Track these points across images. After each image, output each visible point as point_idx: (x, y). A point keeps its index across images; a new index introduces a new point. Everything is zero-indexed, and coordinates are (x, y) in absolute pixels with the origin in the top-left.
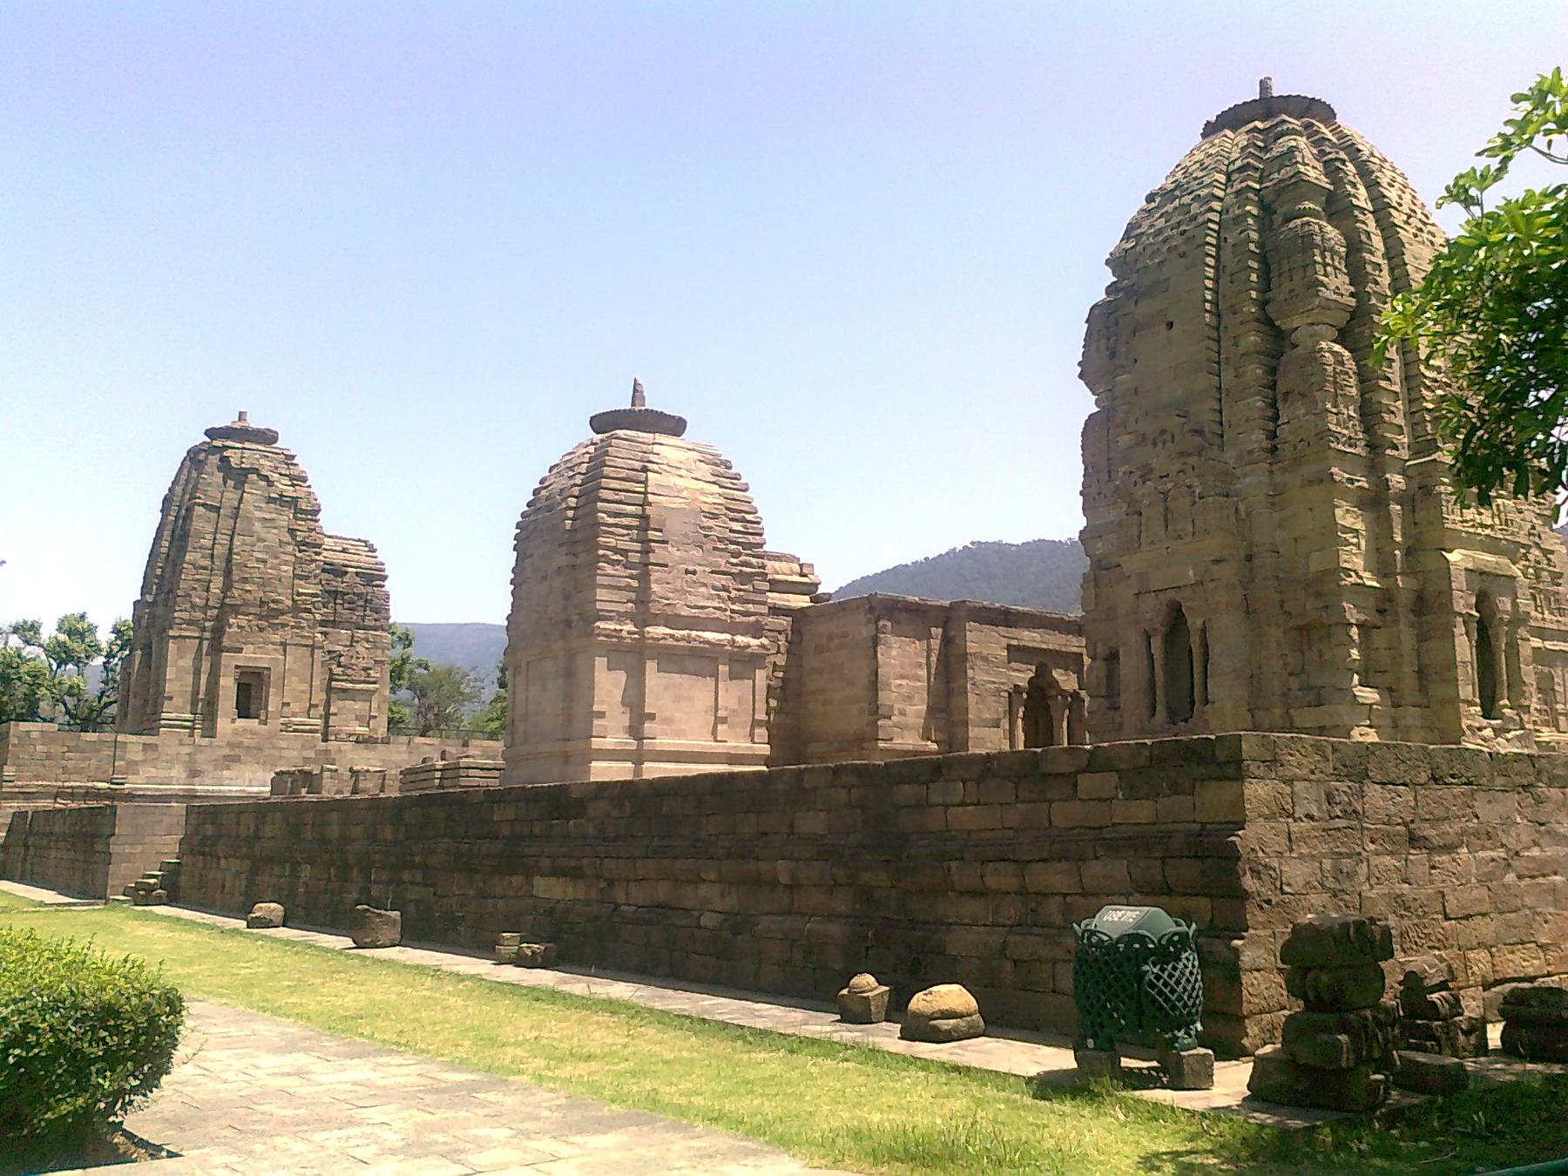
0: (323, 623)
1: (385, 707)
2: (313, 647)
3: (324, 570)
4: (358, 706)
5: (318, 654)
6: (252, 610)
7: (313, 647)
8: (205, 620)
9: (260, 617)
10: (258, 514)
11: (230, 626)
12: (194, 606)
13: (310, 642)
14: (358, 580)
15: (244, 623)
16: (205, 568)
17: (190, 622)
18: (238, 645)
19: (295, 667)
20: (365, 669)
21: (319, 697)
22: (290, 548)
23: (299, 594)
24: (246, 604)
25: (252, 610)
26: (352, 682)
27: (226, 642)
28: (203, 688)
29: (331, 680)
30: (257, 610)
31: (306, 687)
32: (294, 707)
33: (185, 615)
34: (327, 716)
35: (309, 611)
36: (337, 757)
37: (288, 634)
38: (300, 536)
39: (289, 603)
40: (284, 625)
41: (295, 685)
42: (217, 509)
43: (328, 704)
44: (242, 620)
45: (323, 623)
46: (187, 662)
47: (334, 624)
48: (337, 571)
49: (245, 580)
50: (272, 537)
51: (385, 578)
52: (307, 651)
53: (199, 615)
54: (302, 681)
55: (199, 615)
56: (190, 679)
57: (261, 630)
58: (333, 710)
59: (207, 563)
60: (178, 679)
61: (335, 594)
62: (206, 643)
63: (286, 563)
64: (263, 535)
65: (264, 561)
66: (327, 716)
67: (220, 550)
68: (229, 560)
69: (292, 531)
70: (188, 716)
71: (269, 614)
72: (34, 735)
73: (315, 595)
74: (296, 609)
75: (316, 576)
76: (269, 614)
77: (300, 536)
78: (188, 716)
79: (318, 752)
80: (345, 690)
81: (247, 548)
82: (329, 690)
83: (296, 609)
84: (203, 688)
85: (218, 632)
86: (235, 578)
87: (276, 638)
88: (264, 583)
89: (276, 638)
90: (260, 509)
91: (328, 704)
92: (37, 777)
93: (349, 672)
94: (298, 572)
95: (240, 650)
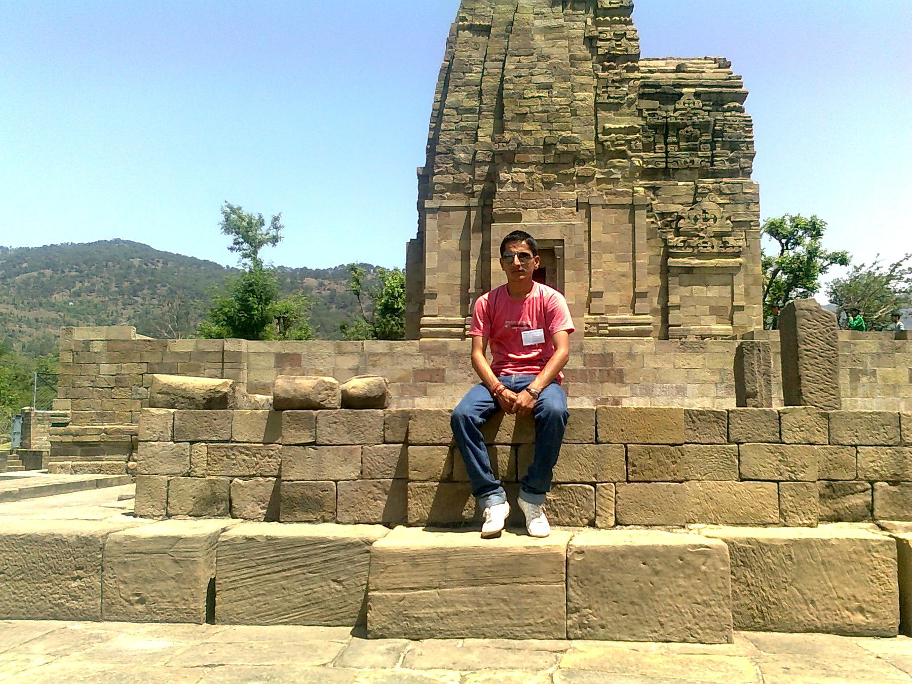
0: (648, 173)
1: (758, 292)
2: (633, 208)
3: (642, 96)
4: (714, 292)
5: (641, 215)
6: (532, 157)
7: (633, 208)
8: (473, 182)
9: (545, 166)
10: (537, 23)
11: (503, 184)
12: (457, 164)
13: (627, 200)
14: (699, 103)
15: (522, 178)
16: (470, 110)
17: (456, 188)
18: (512, 210)
19: (607, 238)
20: (719, 235)
21: (651, 282)
22: (588, 66)
23: (607, 132)
24: (522, 148)
25: (532, 157)
26: (700, 255)
27: (498, 207)
28: (473, 278)
29: (667, 255)
30: (539, 157)
31: (626, 267)
32: (611, 298)
33: (448, 179)
34: (665, 311)
35: (622, 155)
36: (627, 366)
37: (594, 192)
38: (603, 47)
39: (591, 145)
40: (584, 179)
41: (608, 265)
42: (485, 30)
43: (665, 292)
44: (520, 174)
45: (648, 173)
46: (452, 244)
47: (666, 173)
48: (668, 95)
49: (523, 117)
50: (559, 52)
51: (743, 96)
52: (624, 215)
53: (466, 176)
54: (620, 259)
55: (466, 176)
56: (456, 267)
57: (548, 185)
58: (674, 299)
59: (474, 103)
60: (442, 268)
61: (664, 129)
62: (473, 213)
63: (583, 87)
64: (546, 51)
65: (549, 87)
66: (665, 311)
67: (490, 83)
68: (500, 96)
69: (590, 41)
70: (459, 319)
71: (560, 161)
72: (97, 347)
73: (631, 130)
74: (603, 154)
75: (631, 103)
76: (560, 161)
77: (603, 47)
78: (459, 319)
79: (589, 359)
80: (689, 270)
81: (523, 72)
82: (666, 271)
83: (603, 154)
84: (473, 278)
85: (488, 196)
86: (508, 115)
87: (572, 195)
88: (550, 118)
89: (572, 195)
90: (543, 16)
91: (665, 292)
92: (102, 416)
93: (695, 241)
94: (603, 99)
95: (518, 217)
